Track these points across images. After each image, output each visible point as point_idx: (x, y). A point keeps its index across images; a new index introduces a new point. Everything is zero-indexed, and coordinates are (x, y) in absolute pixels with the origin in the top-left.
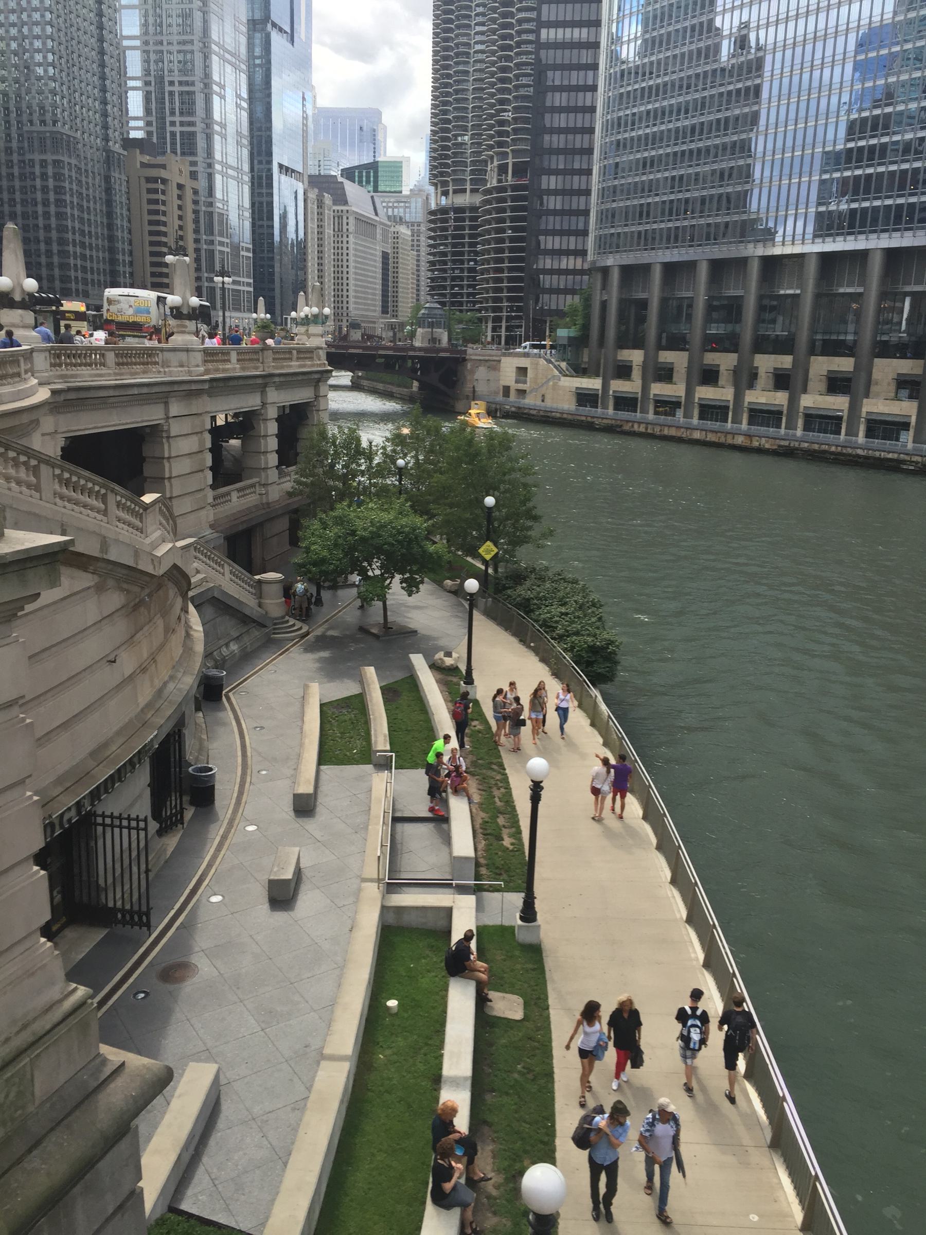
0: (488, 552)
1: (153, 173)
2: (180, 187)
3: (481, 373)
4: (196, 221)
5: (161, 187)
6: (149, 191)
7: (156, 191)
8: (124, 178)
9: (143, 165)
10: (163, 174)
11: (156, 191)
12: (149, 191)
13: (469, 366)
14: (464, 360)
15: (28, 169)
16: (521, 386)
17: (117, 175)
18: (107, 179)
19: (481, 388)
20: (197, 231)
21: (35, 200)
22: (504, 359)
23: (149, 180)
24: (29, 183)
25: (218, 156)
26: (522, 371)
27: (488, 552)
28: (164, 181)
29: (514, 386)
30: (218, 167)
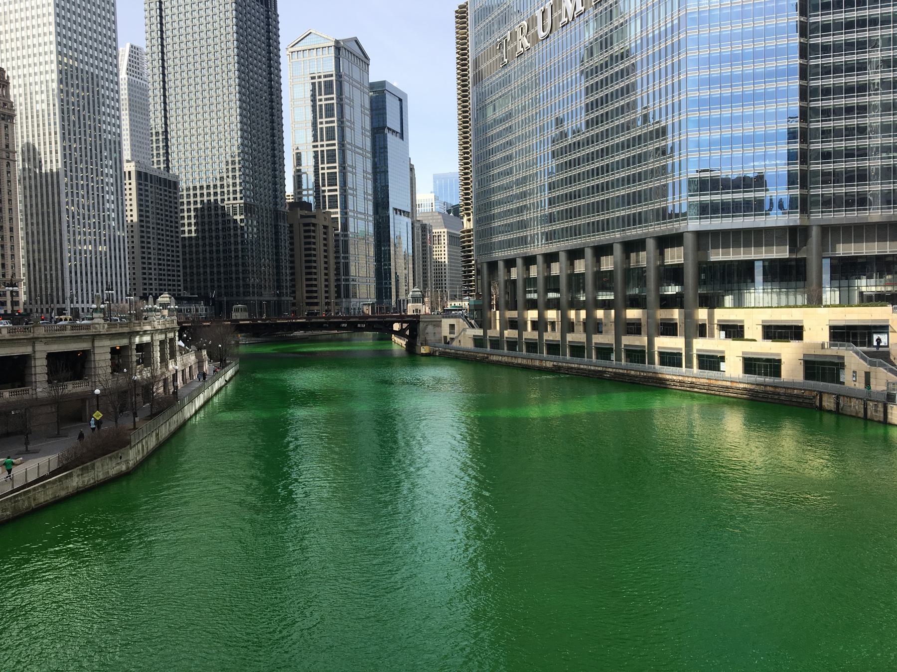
0: (98, 416)
1: (308, 221)
2: (325, 227)
3: (430, 329)
4: (337, 246)
5: (313, 228)
6: (305, 231)
7: (309, 231)
8: (287, 225)
9: (302, 217)
10: (313, 221)
11: (309, 231)
12: (305, 231)
13: (421, 325)
14: (419, 322)
15: (227, 225)
16: (452, 336)
17: (282, 224)
18: (276, 226)
19: (430, 338)
20: (337, 252)
21: (230, 242)
22: (443, 320)
23: (306, 225)
24: (228, 232)
25: (350, 207)
26: (452, 326)
27: (98, 416)
28: (314, 225)
29: (449, 336)
30: (351, 214)
